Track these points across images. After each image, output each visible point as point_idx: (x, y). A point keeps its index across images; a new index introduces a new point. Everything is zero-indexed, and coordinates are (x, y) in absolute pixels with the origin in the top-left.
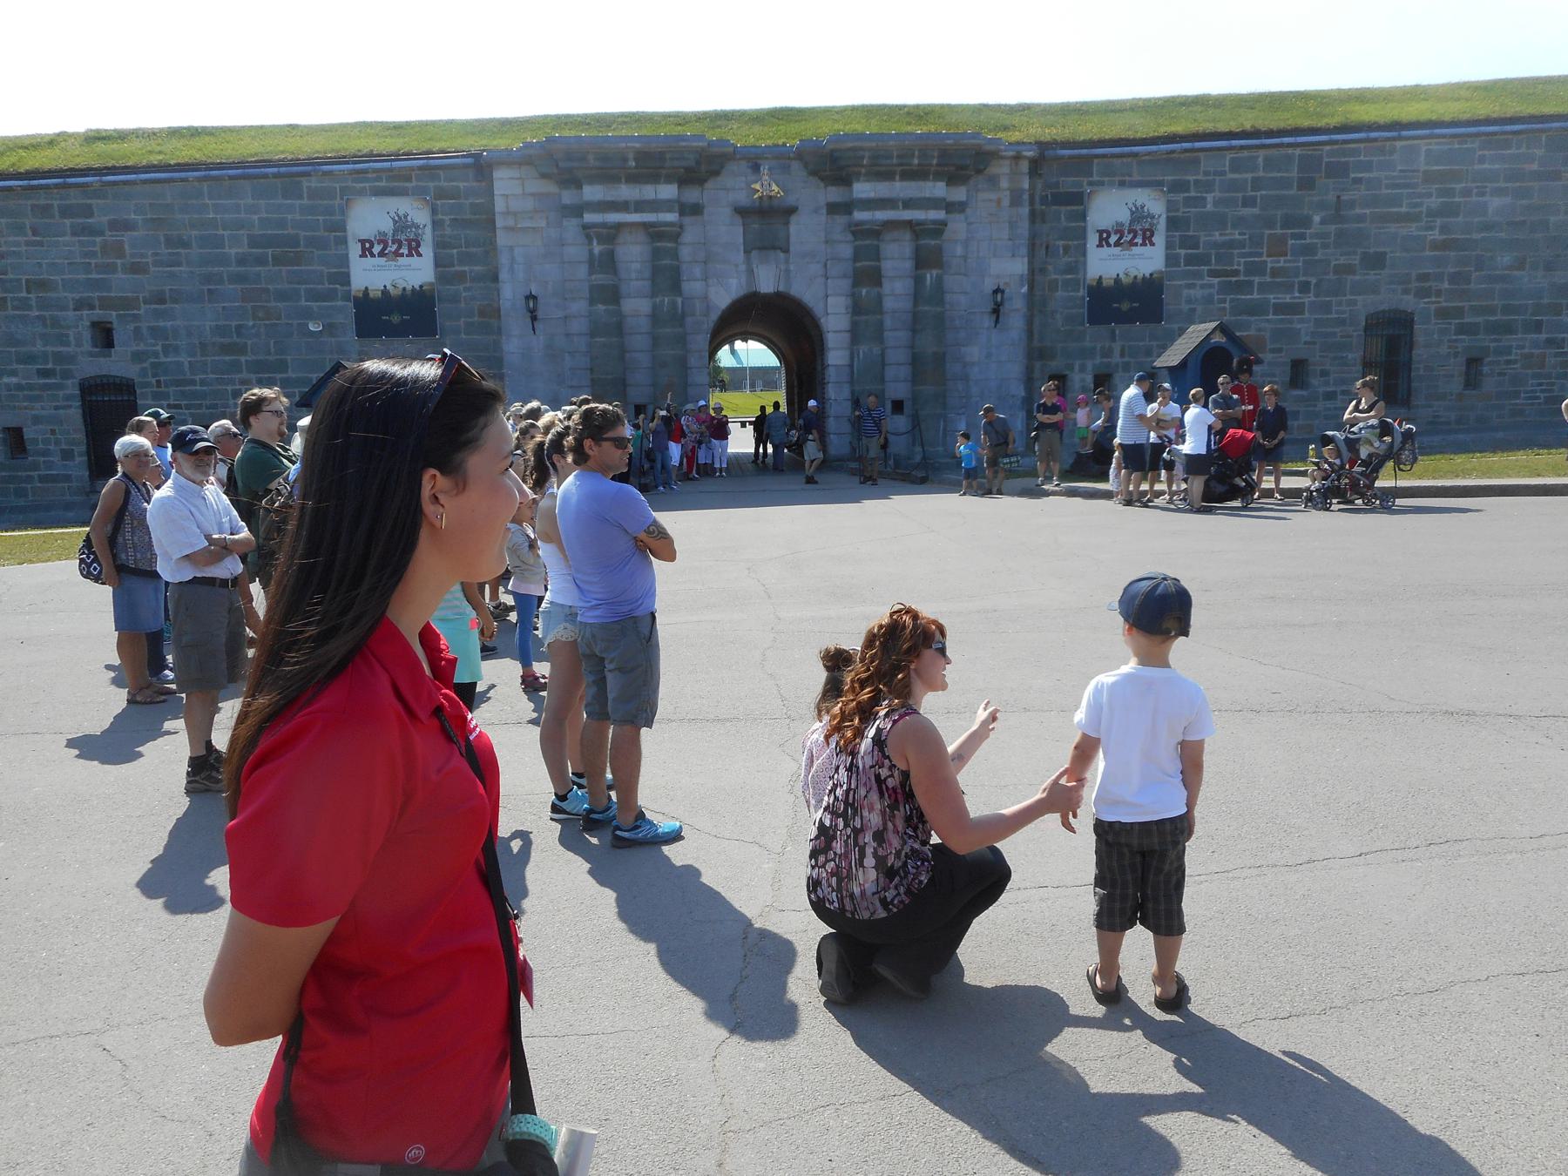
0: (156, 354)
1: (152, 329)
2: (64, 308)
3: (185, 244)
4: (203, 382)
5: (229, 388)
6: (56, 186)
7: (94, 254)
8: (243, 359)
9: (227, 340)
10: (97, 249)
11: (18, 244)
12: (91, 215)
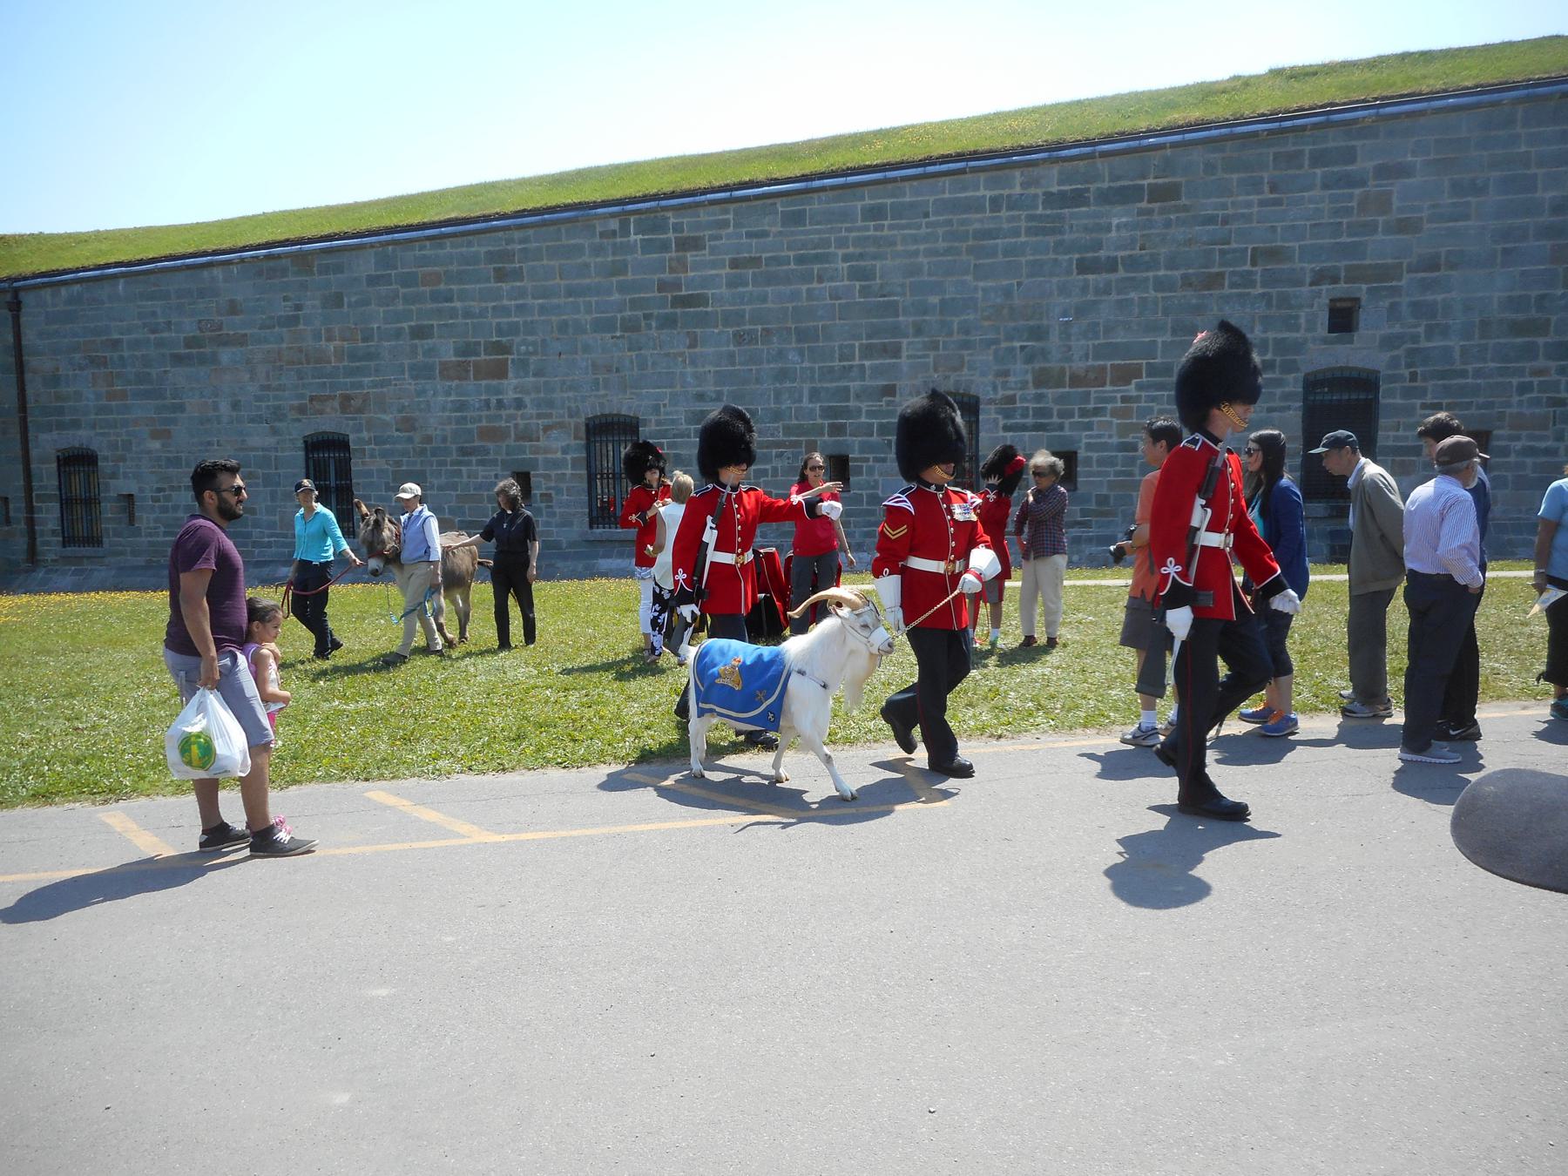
0: (1415, 338)
1: (1415, 306)
2: (1299, 283)
3: (1478, 189)
4: (1478, 373)
5: (1515, 381)
6: (1315, 126)
7: (1348, 211)
8: (1541, 340)
9: (1520, 317)
10: (1354, 204)
11: (1249, 204)
12: (1353, 161)
